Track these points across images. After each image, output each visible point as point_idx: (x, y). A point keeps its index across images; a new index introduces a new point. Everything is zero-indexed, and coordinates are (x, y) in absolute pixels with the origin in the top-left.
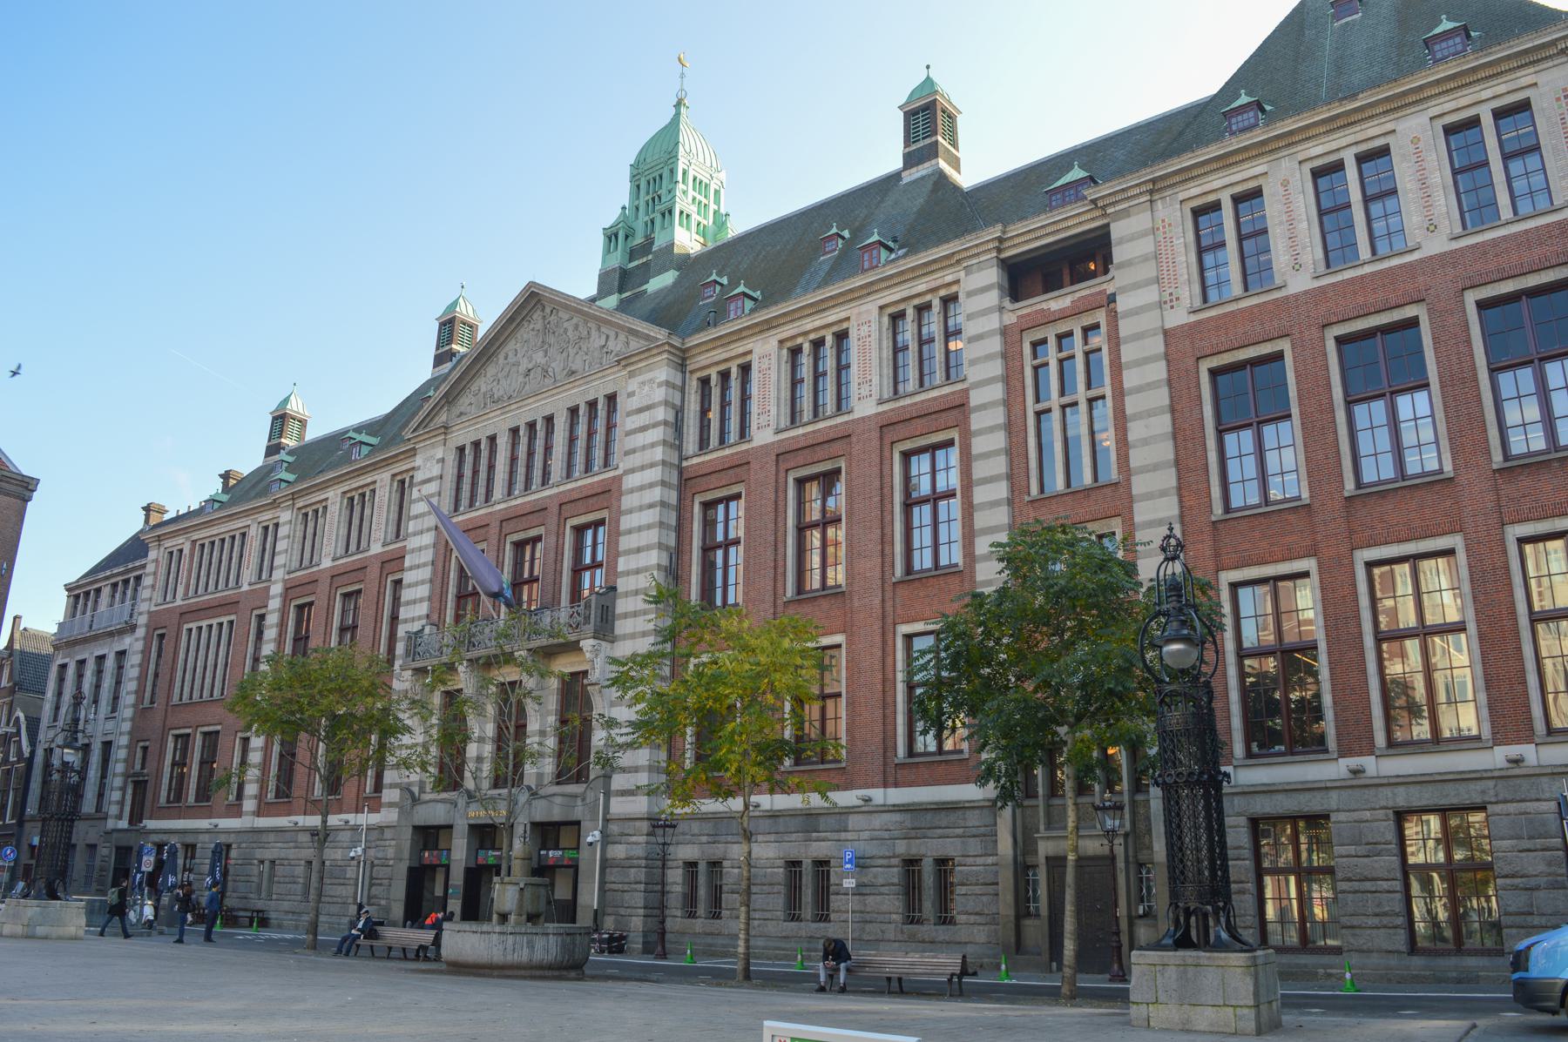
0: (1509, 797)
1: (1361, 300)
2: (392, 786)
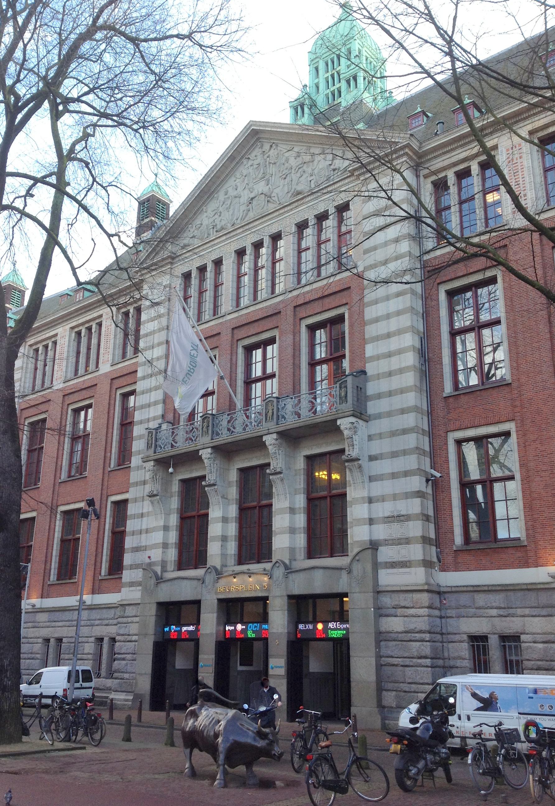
2: (132, 567)
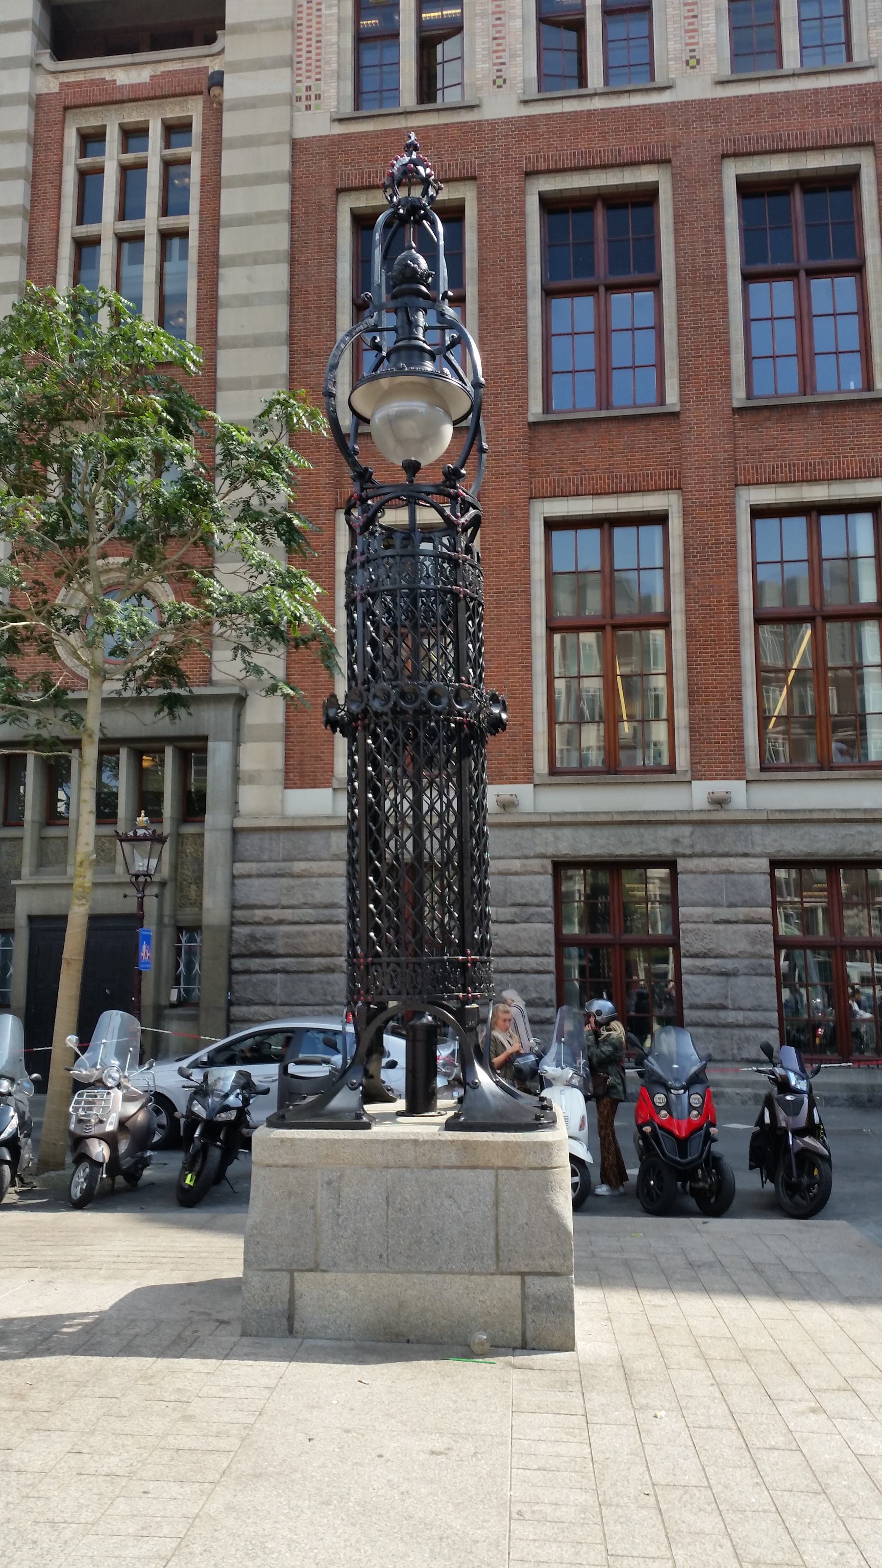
0: (708, 849)
1: (583, 145)
